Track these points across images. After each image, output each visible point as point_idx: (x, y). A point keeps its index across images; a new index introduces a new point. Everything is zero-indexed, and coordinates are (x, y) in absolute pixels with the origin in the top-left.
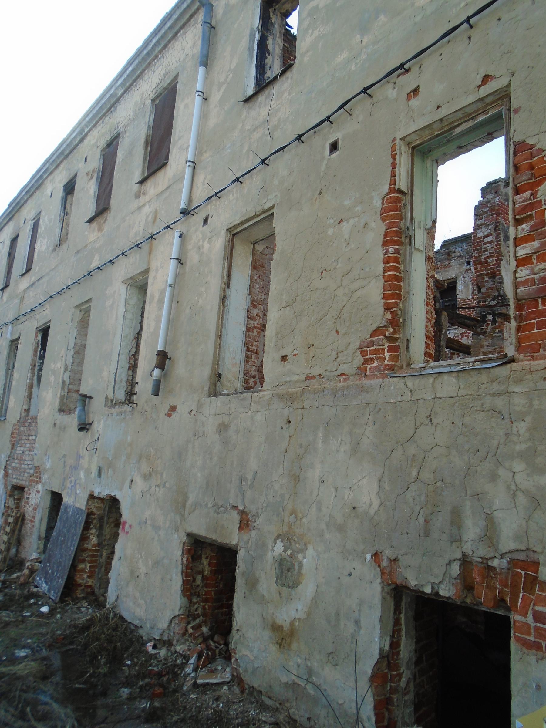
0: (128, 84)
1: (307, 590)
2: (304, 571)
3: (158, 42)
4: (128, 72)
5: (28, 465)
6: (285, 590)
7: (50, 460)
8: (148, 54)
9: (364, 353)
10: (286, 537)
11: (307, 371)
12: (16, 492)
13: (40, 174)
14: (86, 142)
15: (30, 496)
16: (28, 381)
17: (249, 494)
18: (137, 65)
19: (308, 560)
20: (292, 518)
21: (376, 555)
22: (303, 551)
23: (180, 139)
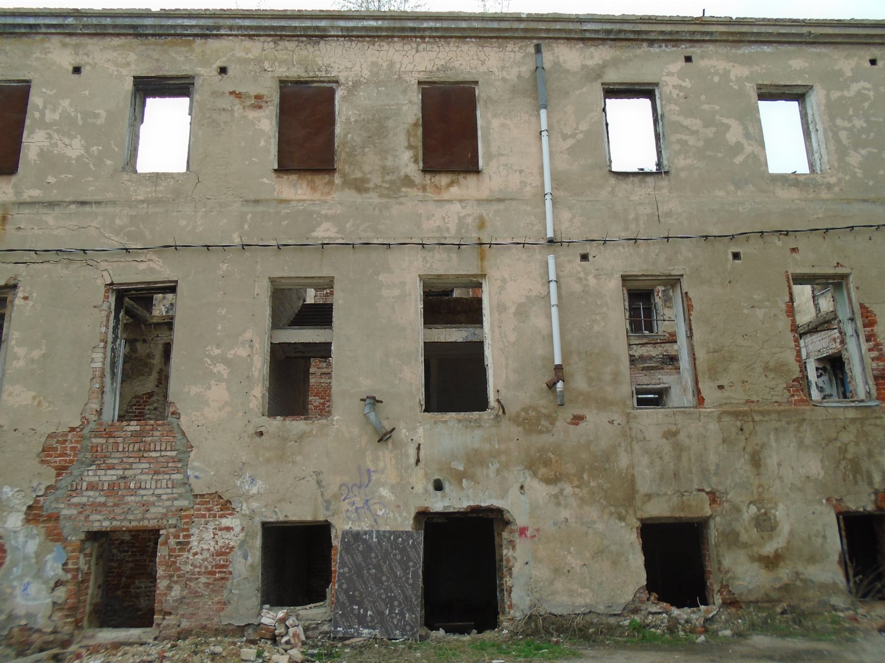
0: (354, 33)
1: (785, 528)
2: (778, 519)
3: (436, 29)
4: (366, 23)
5: (159, 496)
6: (766, 535)
7: (259, 483)
8: (413, 29)
9: (789, 391)
10: (758, 502)
11: (746, 398)
12: (88, 545)
13: (31, 21)
14: (213, 44)
15: (193, 538)
16: (99, 365)
17: (714, 479)
18: (388, 29)
19: (780, 513)
20: (760, 490)
21: (828, 500)
22: (775, 507)
23: (500, 155)
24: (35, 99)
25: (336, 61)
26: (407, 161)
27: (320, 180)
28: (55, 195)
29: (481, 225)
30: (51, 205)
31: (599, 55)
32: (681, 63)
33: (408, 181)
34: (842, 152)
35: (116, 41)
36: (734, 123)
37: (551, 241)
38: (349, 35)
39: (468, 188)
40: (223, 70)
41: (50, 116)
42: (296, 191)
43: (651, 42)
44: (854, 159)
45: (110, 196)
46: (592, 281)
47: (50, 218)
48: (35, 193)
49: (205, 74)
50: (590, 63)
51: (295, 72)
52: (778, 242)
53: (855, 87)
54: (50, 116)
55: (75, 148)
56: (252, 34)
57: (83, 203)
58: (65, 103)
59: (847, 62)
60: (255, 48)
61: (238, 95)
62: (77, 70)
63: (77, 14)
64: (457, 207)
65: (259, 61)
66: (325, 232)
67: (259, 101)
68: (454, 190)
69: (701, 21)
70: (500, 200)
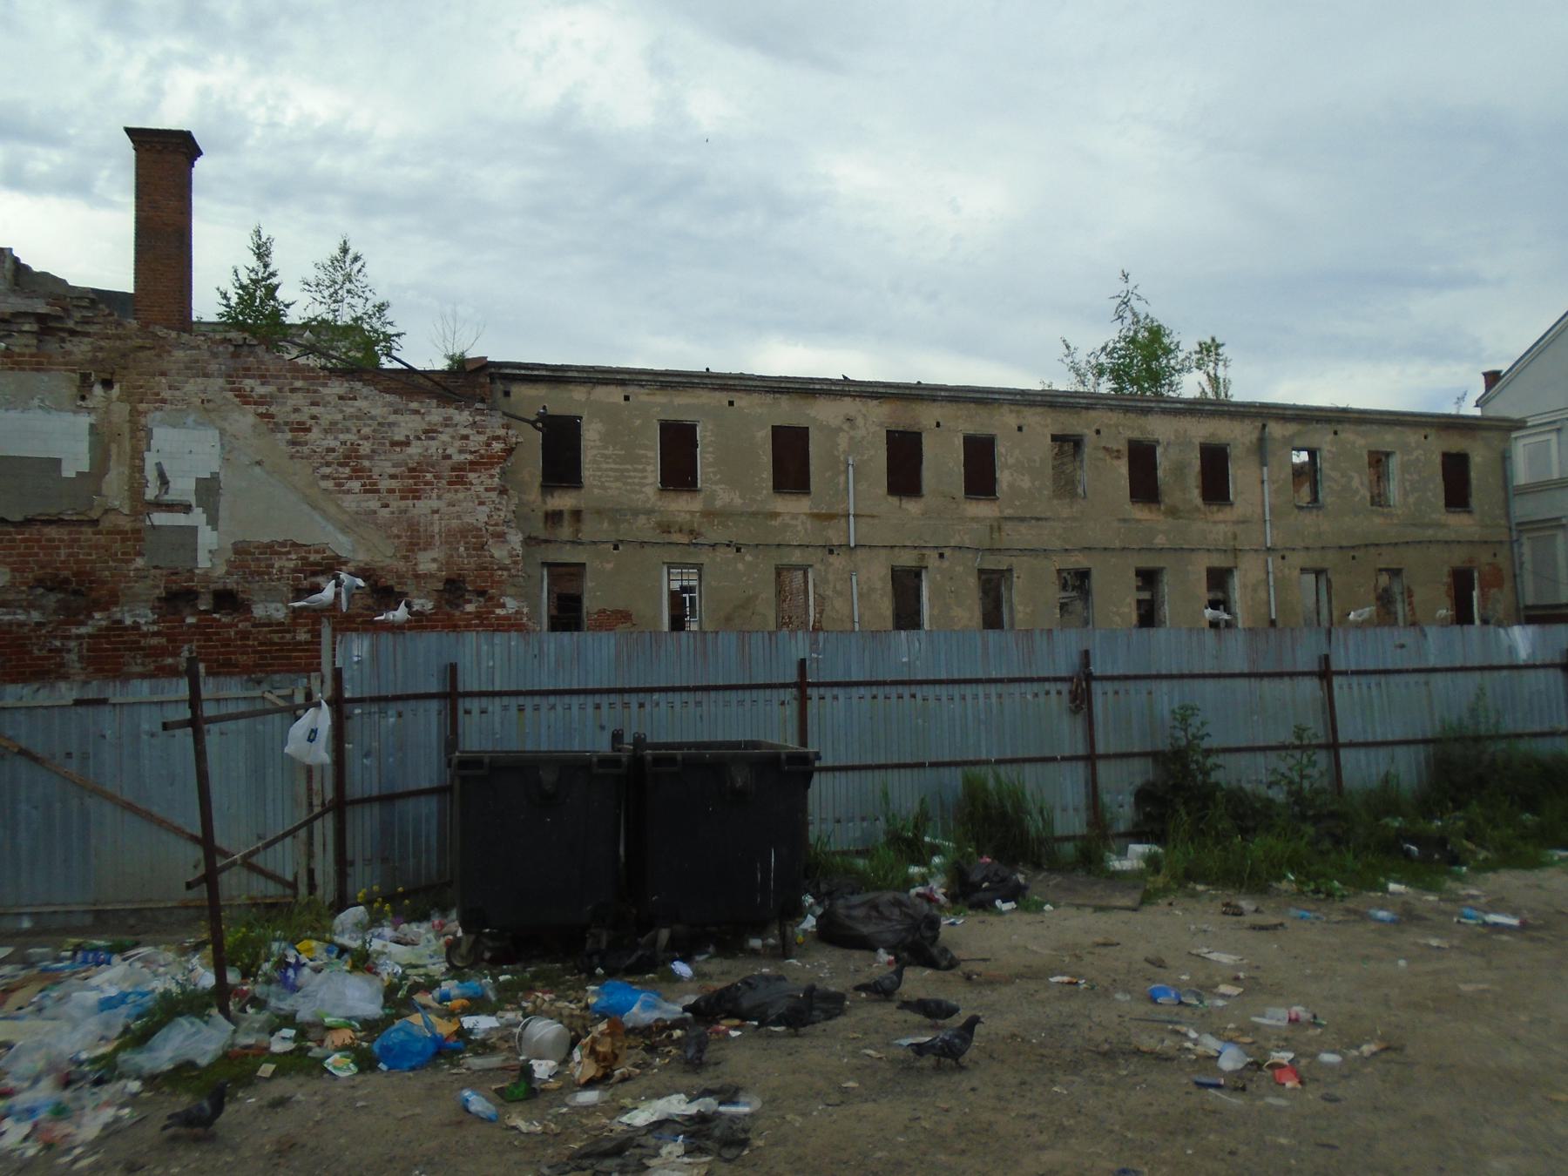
14: (1092, 414)
24: (1000, 449)
25: (1159, 429)
26: (1195, 495)
27: (1154, 507)
28: (1020, 513)
29: (1235, 537)
30: (1022, 519)
31: (1292, 428)
32: (1331, 436)
33: (1198, 509)
34: (1406, 494)
35: (1039, 410)
36: (1355, 475)
37: (1268, 549)
38: (1164, 412)
39: (1226, 514)
40: (1098, 432)
41: (1011, 461)
42: (1141, 513)
43: (1318, 421)
44: (1411, 500)
45: (1048, 514)
46: (1286, 571)
47: (1023, 528)
48: (1009, 512)
49: (1089, 433)
50: (1287, 433)
51: (1136, 435)
52: (1372, 550)
53: (1416, 454)
54: (1011, 461)
55: (1026, 483)
56: (1111, 408)
57: (1038, 519)
58: (1017, 452)
59: (1413, 437)
60: (1115, 417)
61: (1105, 448)
62: (1020, 429)
63: (1023, 393)
64: (1222, 527)
65: (1117, 426)
66: (1160, 540)
67: (1117, 455)
68: (1220, 516)
69: (1345, 410)
70: (1243, 522)
